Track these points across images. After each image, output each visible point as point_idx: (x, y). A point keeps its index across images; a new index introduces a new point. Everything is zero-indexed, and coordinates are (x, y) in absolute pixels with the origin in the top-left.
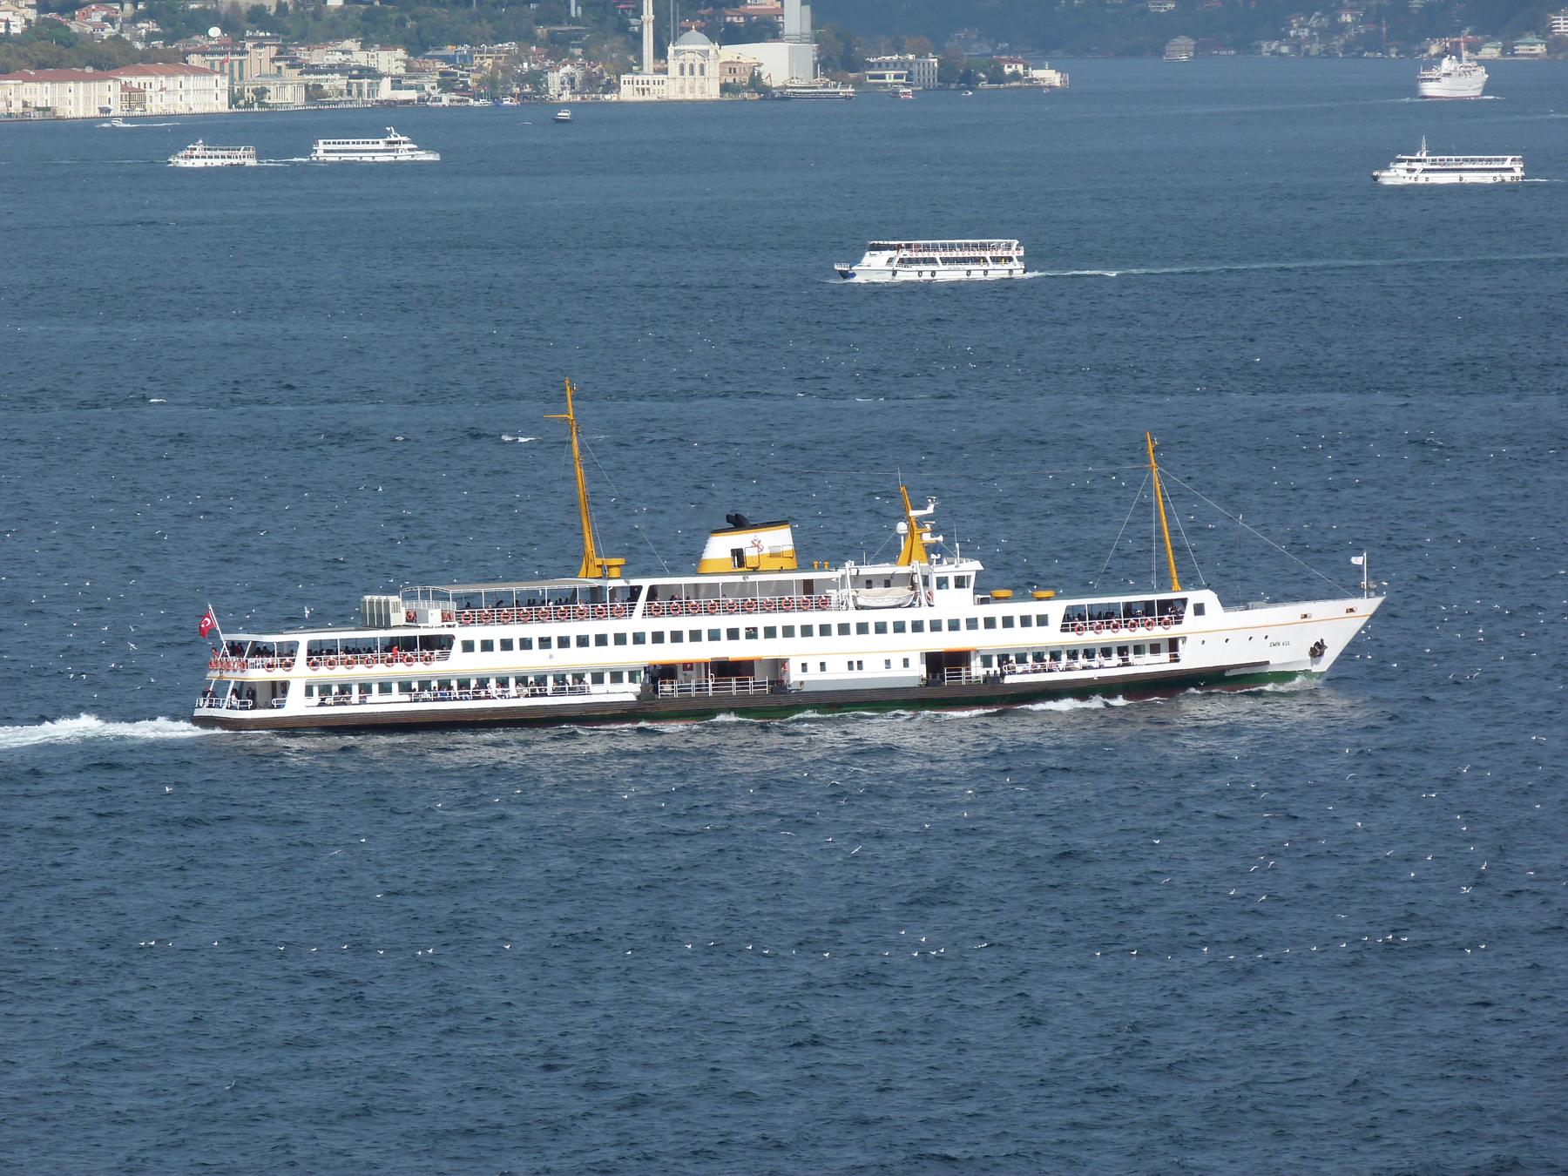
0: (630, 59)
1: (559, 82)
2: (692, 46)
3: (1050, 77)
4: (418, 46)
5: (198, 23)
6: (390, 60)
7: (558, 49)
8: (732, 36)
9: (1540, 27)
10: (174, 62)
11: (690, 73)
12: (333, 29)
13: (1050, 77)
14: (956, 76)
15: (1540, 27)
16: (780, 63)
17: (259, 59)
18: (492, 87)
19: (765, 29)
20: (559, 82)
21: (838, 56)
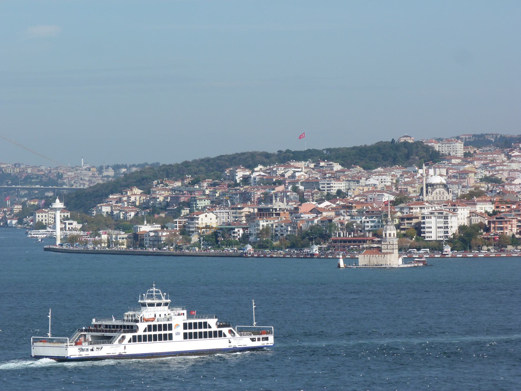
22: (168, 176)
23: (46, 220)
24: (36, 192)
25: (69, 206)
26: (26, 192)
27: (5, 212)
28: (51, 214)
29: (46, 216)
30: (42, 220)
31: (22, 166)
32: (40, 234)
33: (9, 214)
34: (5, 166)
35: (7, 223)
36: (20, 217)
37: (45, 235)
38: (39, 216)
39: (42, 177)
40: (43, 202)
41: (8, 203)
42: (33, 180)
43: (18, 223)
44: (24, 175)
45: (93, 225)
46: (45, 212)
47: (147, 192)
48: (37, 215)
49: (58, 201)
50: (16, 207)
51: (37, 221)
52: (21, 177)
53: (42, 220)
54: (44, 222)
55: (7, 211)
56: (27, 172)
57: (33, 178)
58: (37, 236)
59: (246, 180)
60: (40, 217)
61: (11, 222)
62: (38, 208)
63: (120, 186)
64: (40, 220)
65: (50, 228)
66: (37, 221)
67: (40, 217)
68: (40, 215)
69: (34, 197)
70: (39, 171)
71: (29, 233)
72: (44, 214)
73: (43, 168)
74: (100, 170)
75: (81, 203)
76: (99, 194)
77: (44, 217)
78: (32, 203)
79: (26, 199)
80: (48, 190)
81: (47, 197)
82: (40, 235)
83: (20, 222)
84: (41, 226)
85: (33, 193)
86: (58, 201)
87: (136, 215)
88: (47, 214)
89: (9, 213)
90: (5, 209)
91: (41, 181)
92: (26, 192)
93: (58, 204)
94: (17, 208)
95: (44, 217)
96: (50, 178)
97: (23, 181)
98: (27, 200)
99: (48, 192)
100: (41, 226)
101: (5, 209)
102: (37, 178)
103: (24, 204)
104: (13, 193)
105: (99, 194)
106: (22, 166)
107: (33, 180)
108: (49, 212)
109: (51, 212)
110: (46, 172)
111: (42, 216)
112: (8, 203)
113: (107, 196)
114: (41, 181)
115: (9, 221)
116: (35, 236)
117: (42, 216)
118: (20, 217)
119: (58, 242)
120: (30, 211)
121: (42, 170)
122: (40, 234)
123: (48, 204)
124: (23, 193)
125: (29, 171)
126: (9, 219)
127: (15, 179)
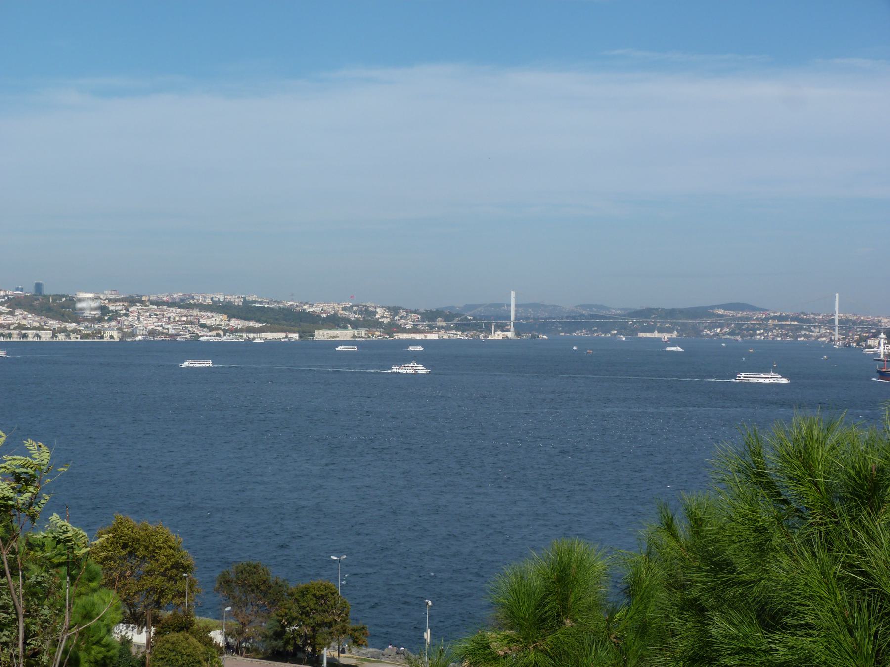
0: (491, 334)
1: (481, 336)
2: (499, 332)
3: (545, 337)
4: (463, 331)
5: (434, 328)
6: (459, 333)
7: (481, 332)
8: (504, 331)
9: (610, 333)
10: (431, 332)
11: (498, 336)
12: (452, 329)
13: (545, 337)
14: (533, 337)
15: (610, 333)
16: (510, 335)
17: (442, 332)
18: (472, 337)
19: (508, 330)
20: (481, 336)
21: (518, 334)
28: (876, 341)
32: (871, 351)
36: (858, 342)
60: (870, 342)
62: (868, 338)
67: (870, 342)
83: (858, 345)
84: (870, 347)
93: (882, 336)
94: (856, 338)
100: (870, 347)
118: (858, 342)
120: (866, 339)
122: (871, 351)
127: (854, 322)
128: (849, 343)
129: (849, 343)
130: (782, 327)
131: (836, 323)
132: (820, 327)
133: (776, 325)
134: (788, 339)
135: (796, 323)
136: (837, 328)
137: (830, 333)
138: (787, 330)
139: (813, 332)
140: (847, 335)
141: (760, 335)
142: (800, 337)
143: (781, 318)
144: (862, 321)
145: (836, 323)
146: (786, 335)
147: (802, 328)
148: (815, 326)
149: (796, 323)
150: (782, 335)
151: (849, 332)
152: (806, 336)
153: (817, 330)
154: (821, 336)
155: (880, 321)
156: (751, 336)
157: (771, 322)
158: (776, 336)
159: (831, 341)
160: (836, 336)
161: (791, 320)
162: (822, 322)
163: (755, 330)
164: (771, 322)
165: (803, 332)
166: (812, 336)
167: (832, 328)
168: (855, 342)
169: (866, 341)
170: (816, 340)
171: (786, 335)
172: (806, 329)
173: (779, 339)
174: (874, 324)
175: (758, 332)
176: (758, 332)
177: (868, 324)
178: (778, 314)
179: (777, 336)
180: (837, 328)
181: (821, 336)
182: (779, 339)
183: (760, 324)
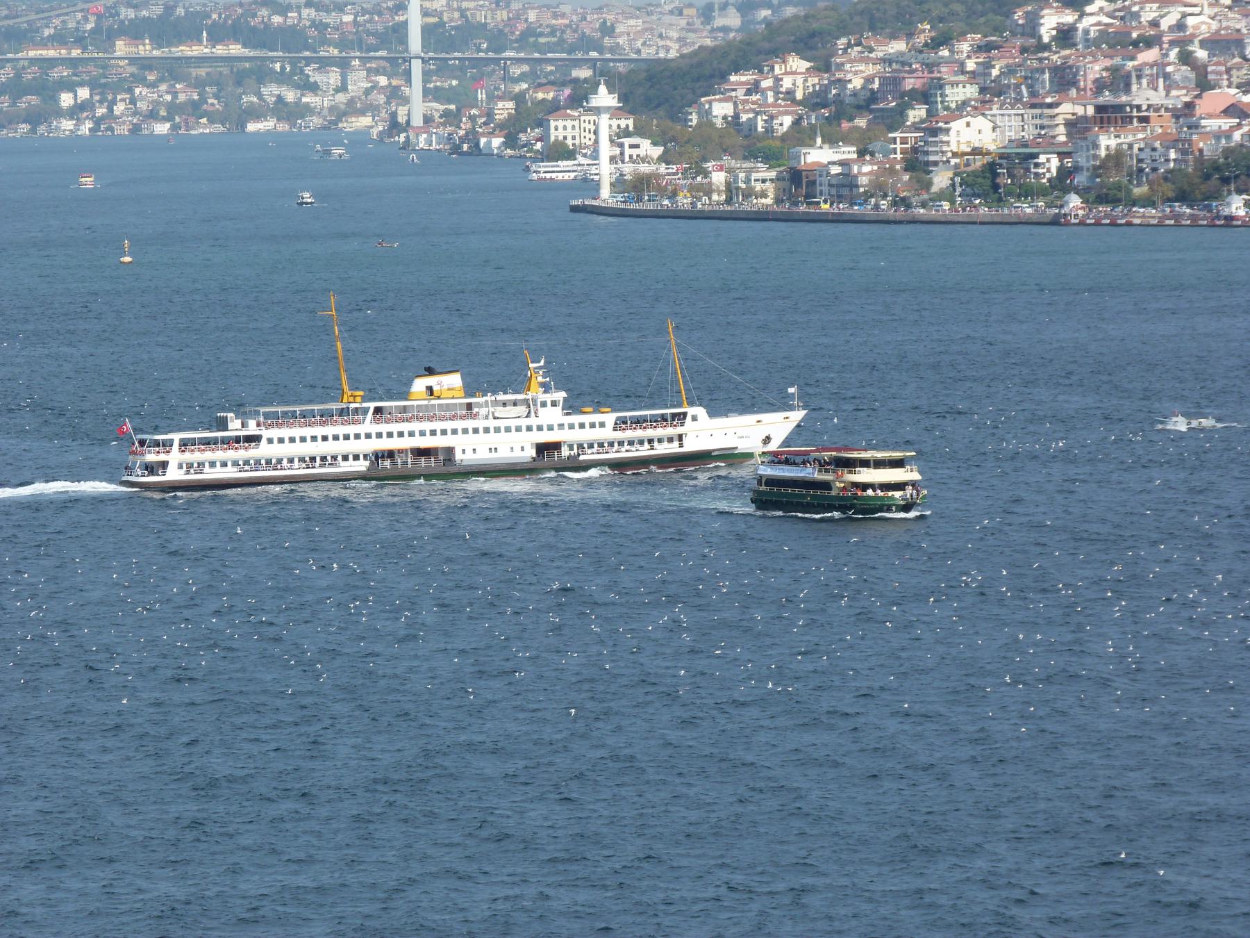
22: (872, 28)
23: (574, 138)
24: (549, 68)
25: (629, 104)
26: (526, 68)
27: (473, 119)
29: (573, 127)
30: (565, 138)
31: (515, 6)
32: (562, 171)
33: (485, 124)
34: (472, 5)
35: (477, 144)
37: (572, 175)
38: (556, 129)
39: (563, 32)
40: (567, 91)
41: (482, 95)
42: (542, 40)
43: (506, 145)
44: (521, 27)
45: (692, 149)
46: (573, 118)
47: (824, 65)
48: (553, 124)
49: (602, 89)
50: (500, 105)
51: (552, 139)
52: (513, 33)
53: (565, 138)
54: (569, 142)
55: (480, 116)
56: (526, 20)
57: (541, 35)
58: (554, 175)
59: (1065, 35)
60: (561, 129)
61: (489, 143)
62: (554, 108)
63: (753, 53)
64: (561, 138)
65: (585, 155)
66: (552, 139)
67: (561, 129)
68: (560, 124)
69: (544, 81)
70: (555, 16)
71: (534, 168)
72: (569, 123)
73: (566, 9)
74: (707, 13)
75: (659, 94)
76: (705, 73)
77: (569, 129)
78: (540, 96)
79: (525, 86)
80: (577, 63)
81: (576, 81)
82: (560, 175)
83: (511, 141)
84: (561, 152)
85: (541, 71)
86: (602, 89)
87: (797, 123)
88: (576, 123)
89: (483, 120)
90: (474, 112)
91: (562, 40)
92: (526, 68)
93: (604, 98)
94: (504, 109)
95: (569, 129)
96: (584, 33)
97: (517, 41)
98: (528, 89)
99: (580, 67)
100: (561, 152)
101: (474, 112)
102: (552, 33)
103: (519, 99)
104: (494, 70)
105: (705, 73)
106: (515, 6)
107: (542, 40)
108: (582, 118)
109: (587, 118)
110: (574, 18)
111: (565, 128)
112: (482, 95)
113: (724, 77)
114: (562, 40)
115: (483, 141)
116: (548, 176)
117: (565, 128)
119: (605, 192)
121: (563, 15)
122: (562, 171)
123: (579, 98)
124: (517, 71)
125: (532, 16)
126: (483, 134)
127: (498, 40)
128: (472, 136)
129: (472, 136)
130: (173, 70)
131: (415, 42)
132: (344, 64)
133: (145, 64)
134: (204, 128)
135: (236, 50)
136: (417, 67)
137: (394, 94)
138: (199, 84)
139: (314, 88)
140: (463, 99)
141: (76, 111)
142: (256, 114)
143: (168, 29)
144: (530, 32)
145: (415, 42)
146: (195, 109)
147: (262, 74)
148: (324, 64)
149: (236, 50)
150: (173, 109)
151: (477, 80)
152: (281, 110)
153: (334, 77)
154: (352, 109)
155: (607, 30)
156: (34, 118)
157: (121, 48)
158: (144, 112)
159: (395, 126)
160: (417, 108)
161: (215, 40)
162: (353, 41)
163: (49, 91)
164: (121, 48)
165: (270, 91)
166: (308, 110)
167: (398, 65)
168: (502, 126)
169: (542, 123)
170: (330, 126)
171: (195, 109)
172: (282, 79)
173: (162, 128)
174: (587, 43)
175: (66, 100)
176: (66, 100)
177: (560, 45)
178: (155, 11)
179: (153, 115)
180: (417, 67)
181: (352, 109)
182: (162, 128)
183: (73, 63)
